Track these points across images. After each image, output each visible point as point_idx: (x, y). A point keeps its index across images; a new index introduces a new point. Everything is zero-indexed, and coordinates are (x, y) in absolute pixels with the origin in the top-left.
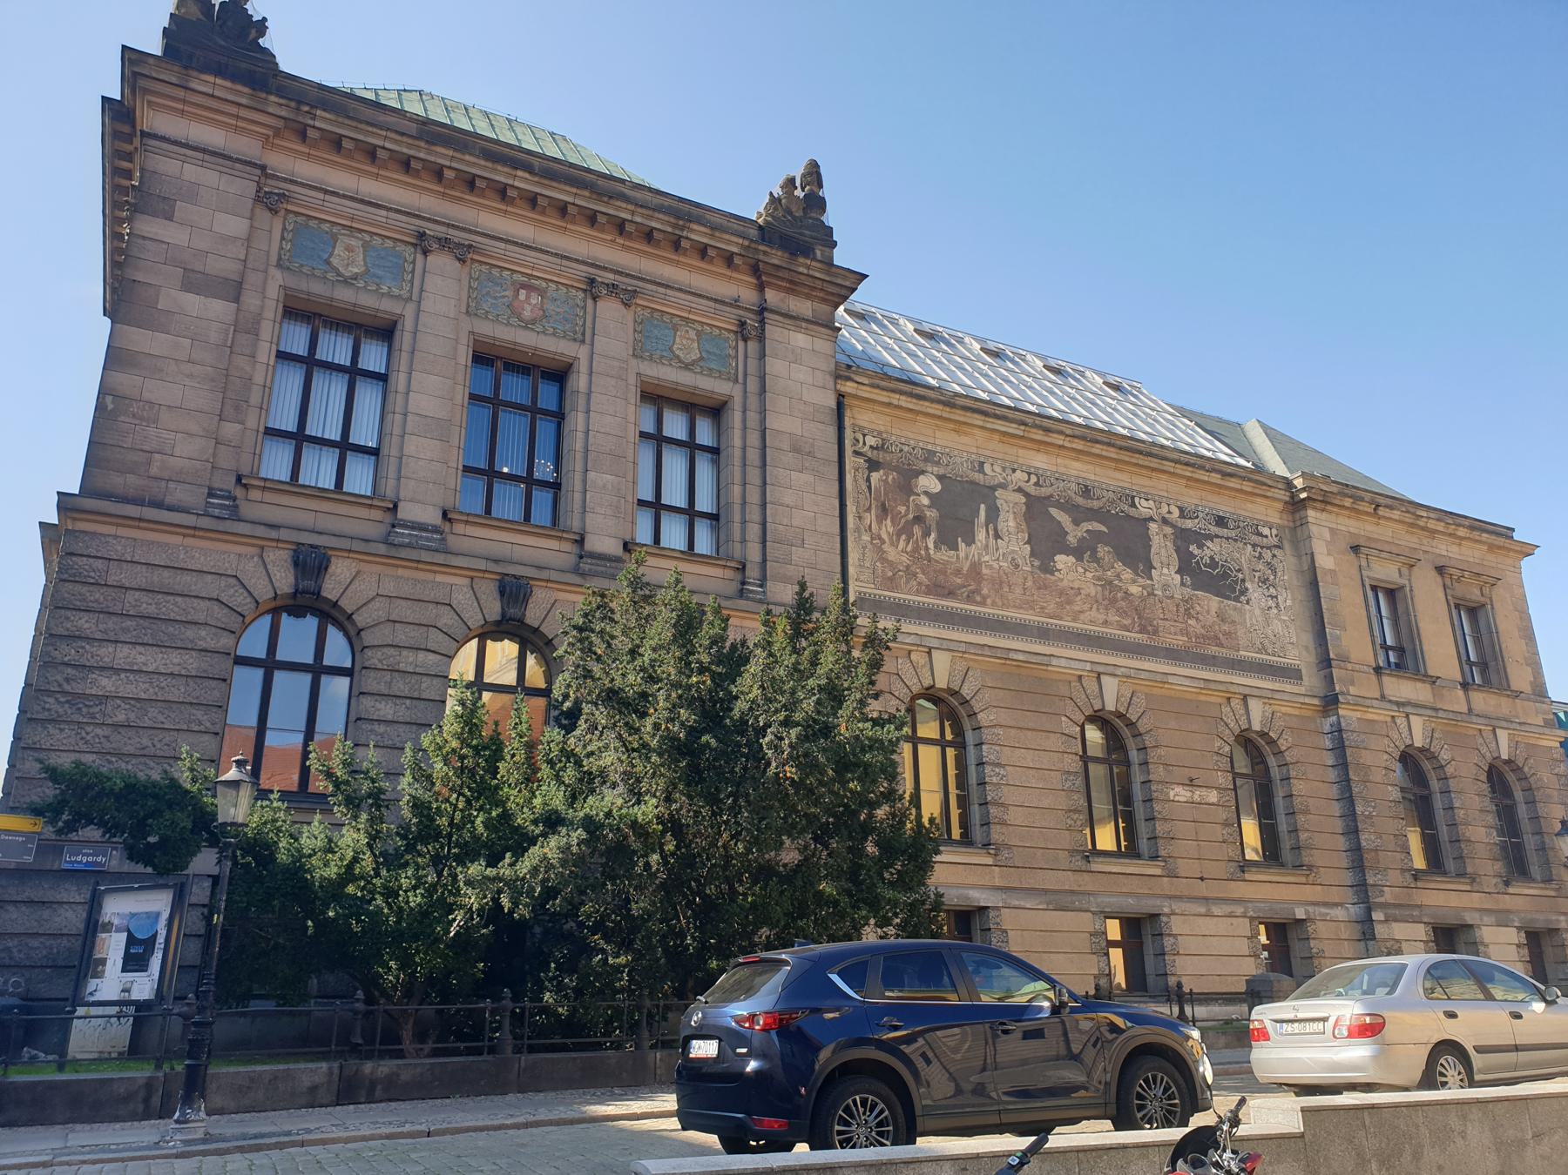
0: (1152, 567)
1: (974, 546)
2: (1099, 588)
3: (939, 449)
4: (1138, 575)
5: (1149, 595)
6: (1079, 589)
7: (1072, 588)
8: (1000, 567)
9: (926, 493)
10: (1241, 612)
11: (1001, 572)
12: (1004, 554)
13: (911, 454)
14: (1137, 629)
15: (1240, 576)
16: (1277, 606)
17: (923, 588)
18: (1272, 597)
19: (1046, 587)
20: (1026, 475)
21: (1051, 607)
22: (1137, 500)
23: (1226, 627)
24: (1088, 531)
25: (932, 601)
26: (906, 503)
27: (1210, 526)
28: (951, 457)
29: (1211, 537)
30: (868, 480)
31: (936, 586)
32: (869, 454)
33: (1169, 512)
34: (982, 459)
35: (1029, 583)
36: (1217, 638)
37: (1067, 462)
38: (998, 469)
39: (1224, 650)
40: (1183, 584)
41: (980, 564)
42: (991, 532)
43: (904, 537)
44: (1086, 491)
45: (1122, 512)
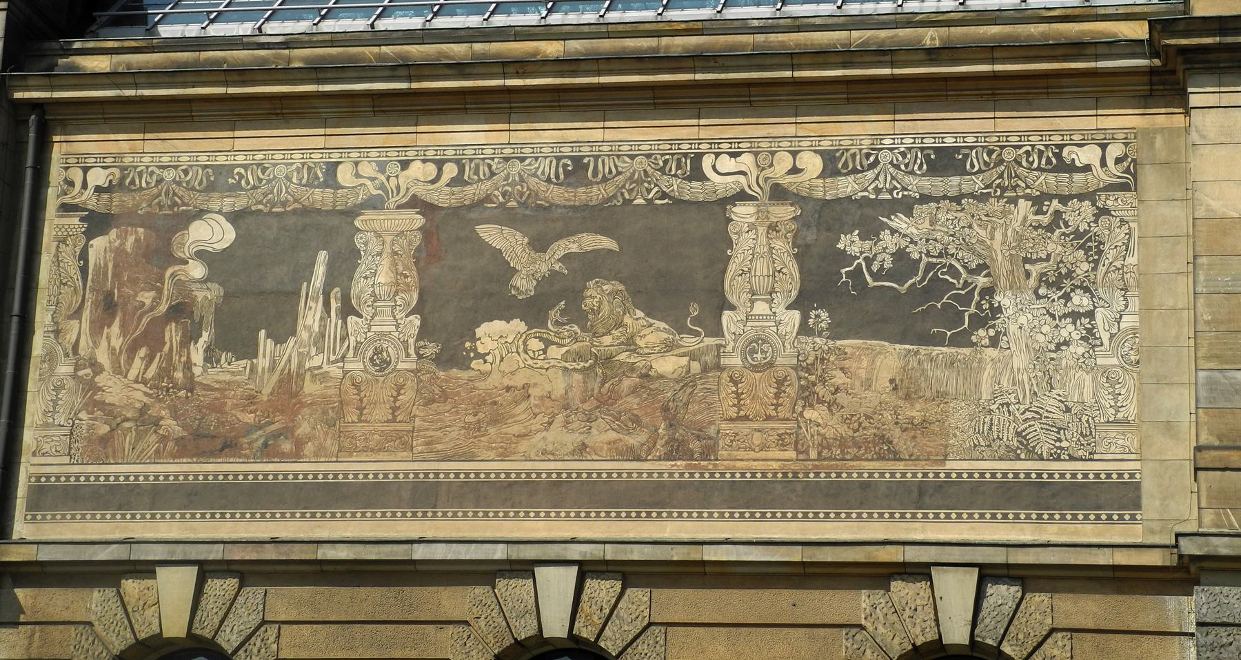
0: (725, 305)
1: (291, 341)
2: (578, 377)
3: (240, 158)
4: (681, 329)
5: (705, 369)
6: (526, 387)
7: (508, 389)
8: (345, 373)
9: (201, 255)
10: (970, 370)
11: (347, 383)
12: (359, 344)
13: (179, 183)
14: (660, 449)
15: (982, 281)
16: (1090, 336)
17: (170, 445)
18: (1075, 316)
19: (445, 396)
20: (432, 169)
21: (453, 436)
22: (707, 162)
23: (915, 412)
24: (567, 258)
25: (185, 468)
26: (156, 284)
27: (908, 179)
28: (264, 170)
29: (906, 206)
30: (84, 256)
31: (197, 435)
32: (92, 205)
33: (795, 170)
34: (335, 157)
35: (406, 397)
36: (883, 439)
38: (367, 169)
39: (900, 466)
40: (805, 329)
41: (301, 376)
42: (334, 305)
43: (143, 352)
45: (664, 195)
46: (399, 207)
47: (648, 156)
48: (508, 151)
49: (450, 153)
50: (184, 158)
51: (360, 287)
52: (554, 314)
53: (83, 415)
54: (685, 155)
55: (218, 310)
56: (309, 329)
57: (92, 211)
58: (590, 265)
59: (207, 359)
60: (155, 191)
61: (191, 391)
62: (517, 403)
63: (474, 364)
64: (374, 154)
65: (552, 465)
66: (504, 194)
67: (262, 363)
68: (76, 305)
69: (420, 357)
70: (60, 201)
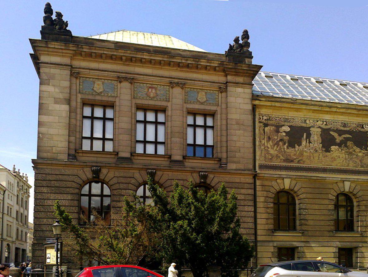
2: (347, 155)
3: (290, 117)
5: (365, 155)
6: (339, 156)
7: (336, 156)
8: (310, 152)
9: (284, 132)
12: (312, 148)
14: (360, 166)
17: (282, 160)
20: (322, 123)
22: (364, 126)
24: (344, 138)
28: (294, 120)
30: (264, 130)
32: (264, 122)
34: (306, 119)
37: (339, 116)
38: (311, 121)
42: (308, 141)
43: (276, 146)
44: (345, 125)
45: (358, 130)
46: (317, 128)
47: (355, 124)
48: (334, 121)
49: (325, 120)
50: (280, 116)
51: (311, 139)
52: (343, 146)
53: (267, 155)
54: (361, 124)
55: (288, 141)
56: (304, 145)
57: (264, 123)
58: (347, 139)
59: (287, 148)
60: (275, 121)
61: (285, 152)
62: (338, 158)
63: (331, 152)
64: (312, 119)
65: (344, 167)
66: (334, 127)
67: (296, 149)
68: (263, 138)
69: (322, 150)
70: (258, 121)
